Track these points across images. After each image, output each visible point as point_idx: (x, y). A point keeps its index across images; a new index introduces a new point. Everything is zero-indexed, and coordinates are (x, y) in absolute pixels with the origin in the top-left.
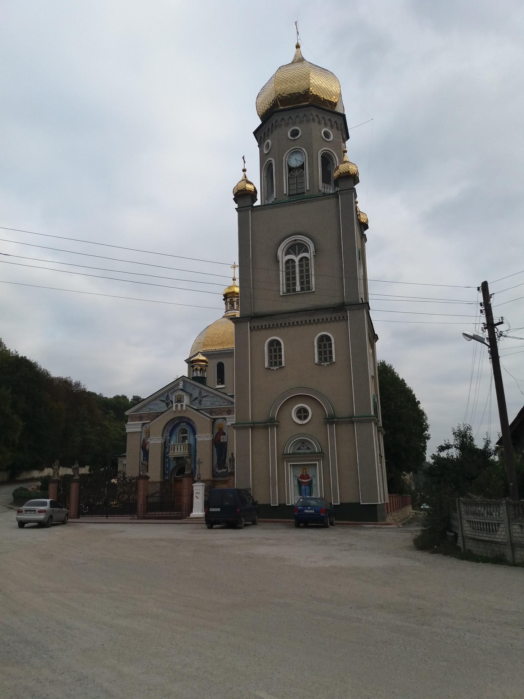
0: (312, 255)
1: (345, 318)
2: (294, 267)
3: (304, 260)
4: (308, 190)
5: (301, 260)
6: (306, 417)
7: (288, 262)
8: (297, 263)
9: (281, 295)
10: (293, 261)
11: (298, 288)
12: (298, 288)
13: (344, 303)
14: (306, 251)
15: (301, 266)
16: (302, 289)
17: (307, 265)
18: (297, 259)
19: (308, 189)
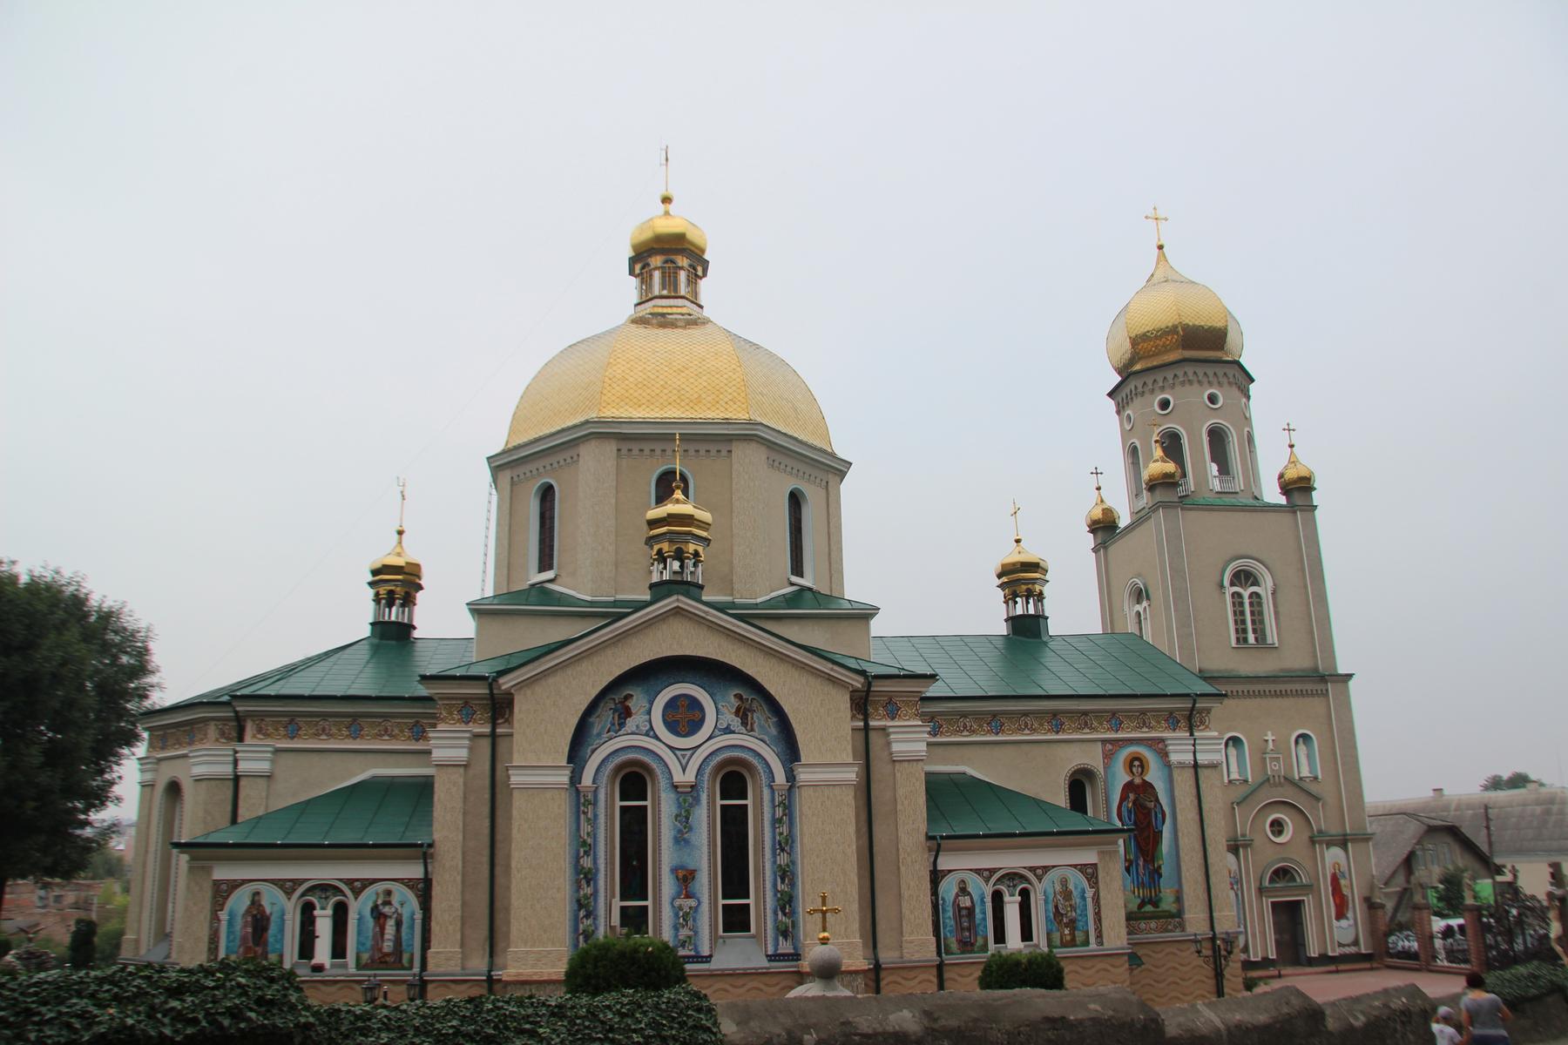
0: (1270, 593)
1: (1324, 692)
2: (1241, 604)
3: (1254, 595)
4: (1242, 491)
5: (1251, 596)
6: (1280, 833)
7: (1234, 595)
8: (1247, 601)
9: (1234, 645)
10: (1239, 595)
11: (1251, 638)
12: (1251, 638)
13: (1316, 669)
14: (1256, 583)
15: (1251, 604)
16: (1256, 639)
17: (1260, 604)
18: (1246, 594)
19: (1242, 488)
